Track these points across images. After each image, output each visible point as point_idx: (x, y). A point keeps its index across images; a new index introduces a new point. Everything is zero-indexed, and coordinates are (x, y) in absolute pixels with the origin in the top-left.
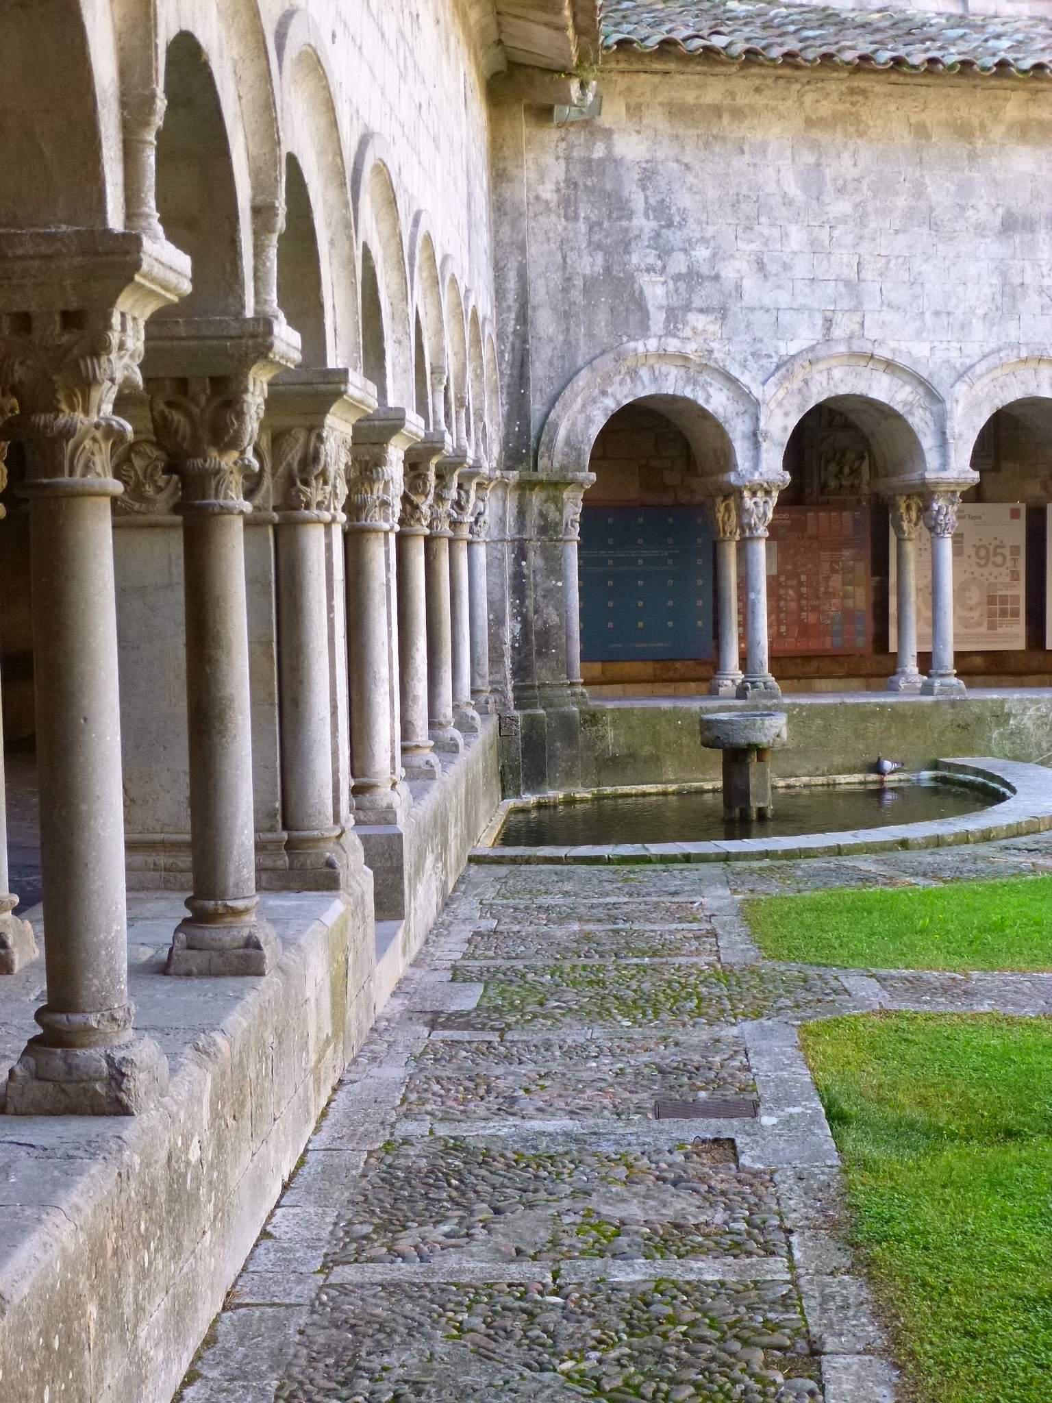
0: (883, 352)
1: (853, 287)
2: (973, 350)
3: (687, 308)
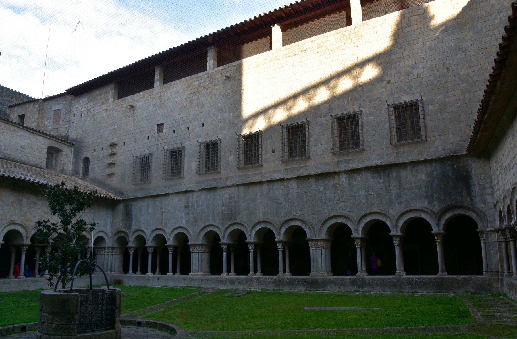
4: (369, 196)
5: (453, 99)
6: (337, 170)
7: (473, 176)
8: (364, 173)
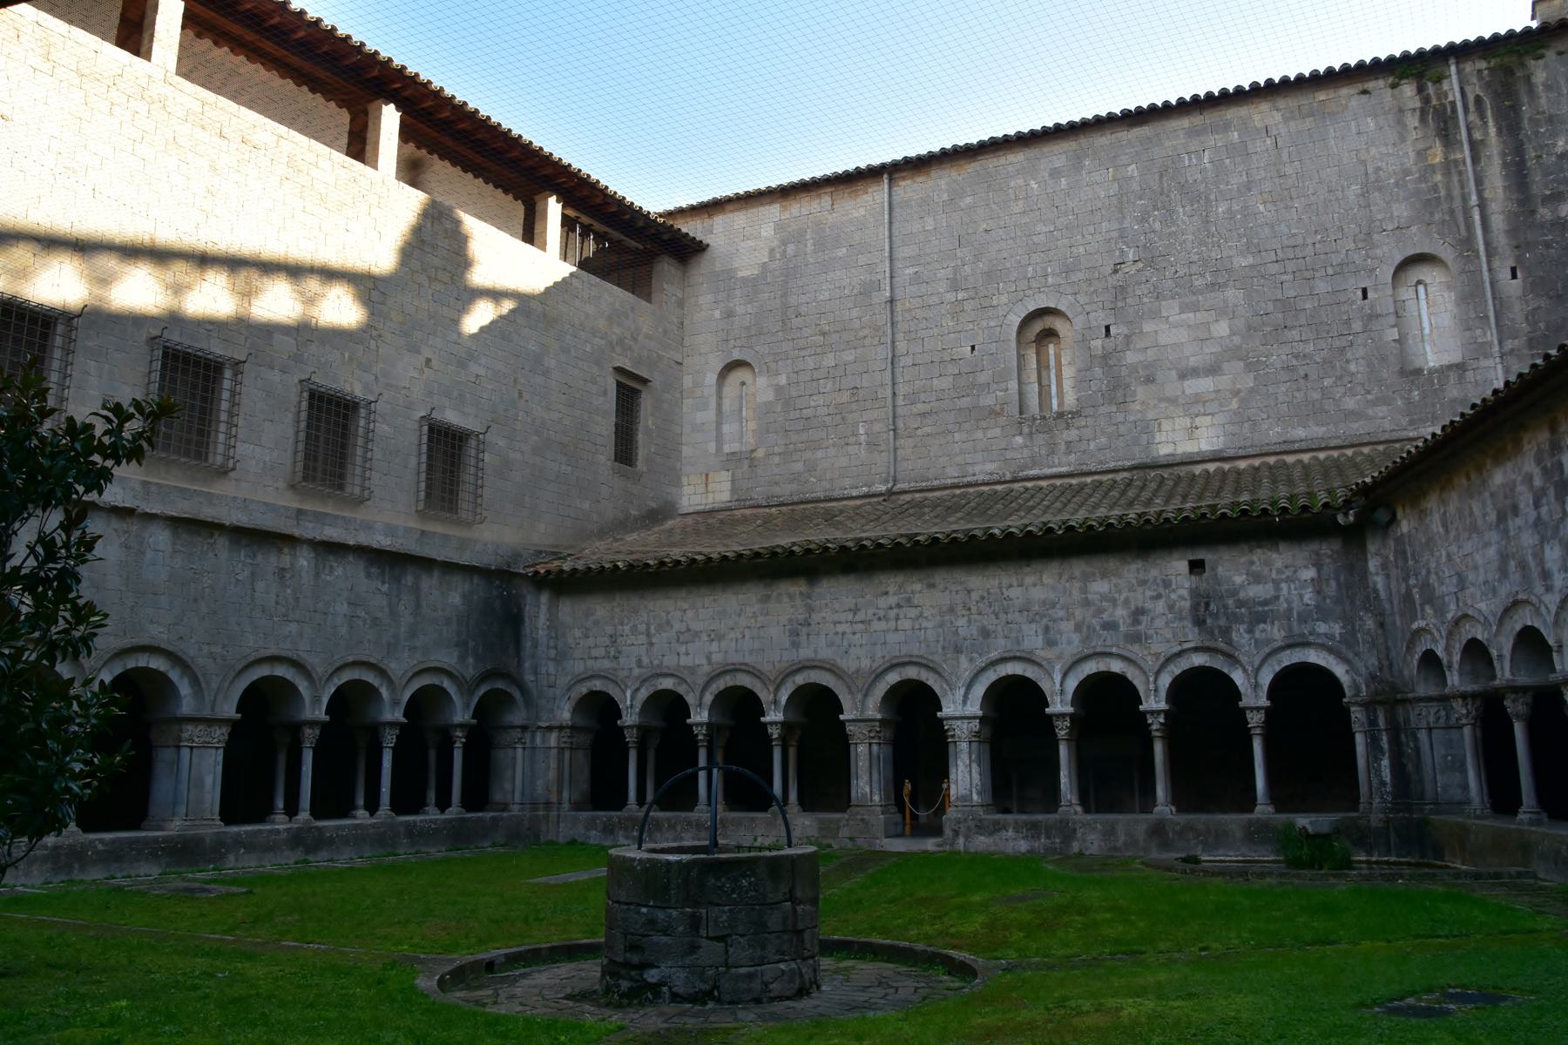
4: (355, 619)
5: (518, 456)
6: (297, 532)
7: (526, 619)
8: (351, 558)
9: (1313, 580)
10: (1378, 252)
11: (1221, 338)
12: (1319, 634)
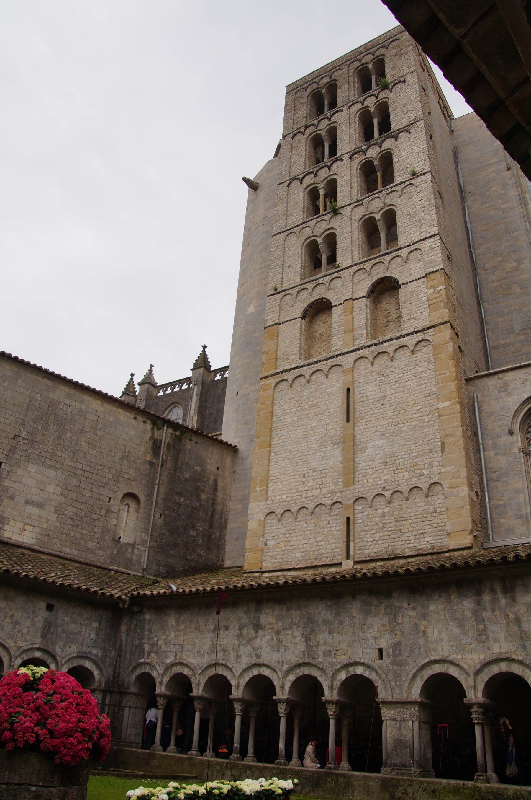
0: (185, 662)
1: (182, 646)
2: (204, 661)
3: (151, 652)
9: (96, 628)
10: (119, 485)
11: (49, 492)
12: (93, 654)
